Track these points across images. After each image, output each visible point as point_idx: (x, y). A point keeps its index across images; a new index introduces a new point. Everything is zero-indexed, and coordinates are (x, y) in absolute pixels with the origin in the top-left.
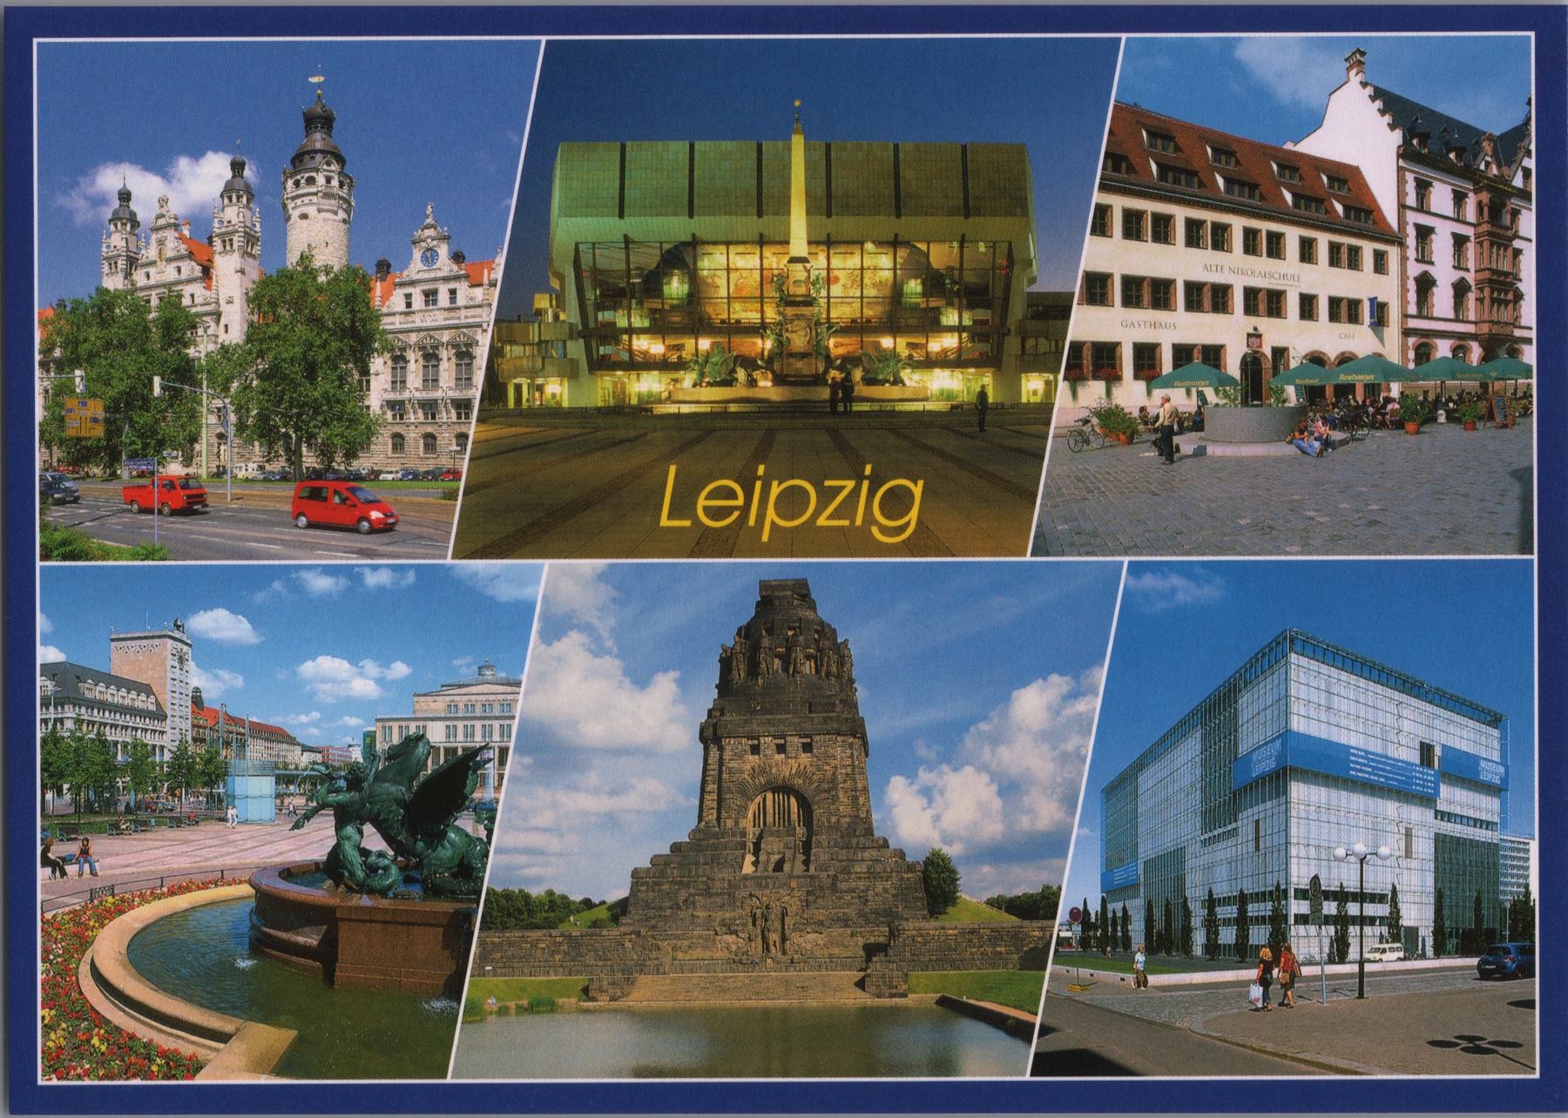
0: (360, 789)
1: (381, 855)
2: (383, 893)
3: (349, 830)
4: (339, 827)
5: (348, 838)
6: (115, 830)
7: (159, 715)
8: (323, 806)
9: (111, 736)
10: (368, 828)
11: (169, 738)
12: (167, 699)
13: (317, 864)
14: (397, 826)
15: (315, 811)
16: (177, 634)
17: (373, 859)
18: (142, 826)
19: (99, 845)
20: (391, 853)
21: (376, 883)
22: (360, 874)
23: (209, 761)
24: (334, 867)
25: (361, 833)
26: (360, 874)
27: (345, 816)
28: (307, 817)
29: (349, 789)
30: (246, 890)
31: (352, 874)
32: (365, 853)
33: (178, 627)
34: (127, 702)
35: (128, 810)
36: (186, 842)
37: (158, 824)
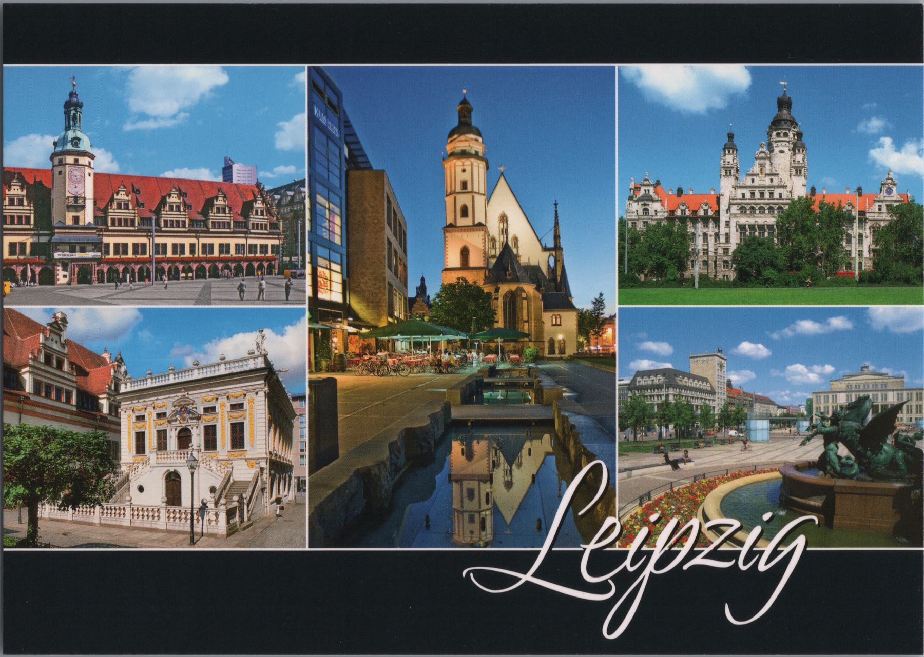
0: (837, 425)
1: (848, 458)
2: (851, 477)
3: (832, 446)
4: (826, 444)
5: (832, 450)
6: (697, 446)
7: (712, 392)
8: (816, 434)
9: (695, 402)
10: (840, 444)
11: (717, 404)
12: (715, 385)
13: (813, 462)
14: (856, 443)
15: (812, 436)
16: (719, 354)
17: (844, 460)
18: (708, 444)
19: (692, 453)
20: (853, 457)
21: (847, 472)
22: (838, 468)
23: (738, 413)
24: (823, 463)
25: (837, 447)
26: (838, 468)
27: (829, 438)
28: (809, 439)
29: (832, 424)
30: (777, 474)
31: (834, 468)
32: (839, 458)
33: (720, 351)
34: (698, 386)
35: (700, 436)
36: (730, 451)
37: (716, 443)
